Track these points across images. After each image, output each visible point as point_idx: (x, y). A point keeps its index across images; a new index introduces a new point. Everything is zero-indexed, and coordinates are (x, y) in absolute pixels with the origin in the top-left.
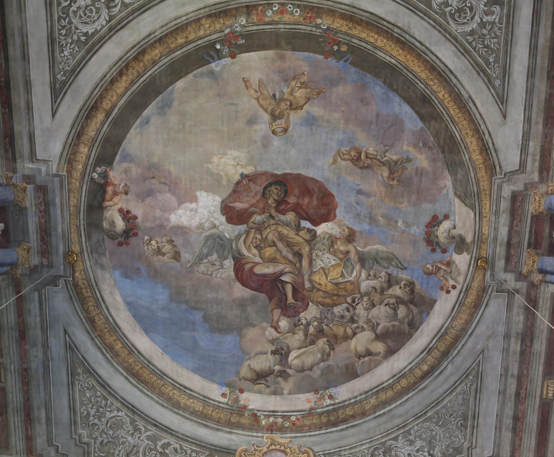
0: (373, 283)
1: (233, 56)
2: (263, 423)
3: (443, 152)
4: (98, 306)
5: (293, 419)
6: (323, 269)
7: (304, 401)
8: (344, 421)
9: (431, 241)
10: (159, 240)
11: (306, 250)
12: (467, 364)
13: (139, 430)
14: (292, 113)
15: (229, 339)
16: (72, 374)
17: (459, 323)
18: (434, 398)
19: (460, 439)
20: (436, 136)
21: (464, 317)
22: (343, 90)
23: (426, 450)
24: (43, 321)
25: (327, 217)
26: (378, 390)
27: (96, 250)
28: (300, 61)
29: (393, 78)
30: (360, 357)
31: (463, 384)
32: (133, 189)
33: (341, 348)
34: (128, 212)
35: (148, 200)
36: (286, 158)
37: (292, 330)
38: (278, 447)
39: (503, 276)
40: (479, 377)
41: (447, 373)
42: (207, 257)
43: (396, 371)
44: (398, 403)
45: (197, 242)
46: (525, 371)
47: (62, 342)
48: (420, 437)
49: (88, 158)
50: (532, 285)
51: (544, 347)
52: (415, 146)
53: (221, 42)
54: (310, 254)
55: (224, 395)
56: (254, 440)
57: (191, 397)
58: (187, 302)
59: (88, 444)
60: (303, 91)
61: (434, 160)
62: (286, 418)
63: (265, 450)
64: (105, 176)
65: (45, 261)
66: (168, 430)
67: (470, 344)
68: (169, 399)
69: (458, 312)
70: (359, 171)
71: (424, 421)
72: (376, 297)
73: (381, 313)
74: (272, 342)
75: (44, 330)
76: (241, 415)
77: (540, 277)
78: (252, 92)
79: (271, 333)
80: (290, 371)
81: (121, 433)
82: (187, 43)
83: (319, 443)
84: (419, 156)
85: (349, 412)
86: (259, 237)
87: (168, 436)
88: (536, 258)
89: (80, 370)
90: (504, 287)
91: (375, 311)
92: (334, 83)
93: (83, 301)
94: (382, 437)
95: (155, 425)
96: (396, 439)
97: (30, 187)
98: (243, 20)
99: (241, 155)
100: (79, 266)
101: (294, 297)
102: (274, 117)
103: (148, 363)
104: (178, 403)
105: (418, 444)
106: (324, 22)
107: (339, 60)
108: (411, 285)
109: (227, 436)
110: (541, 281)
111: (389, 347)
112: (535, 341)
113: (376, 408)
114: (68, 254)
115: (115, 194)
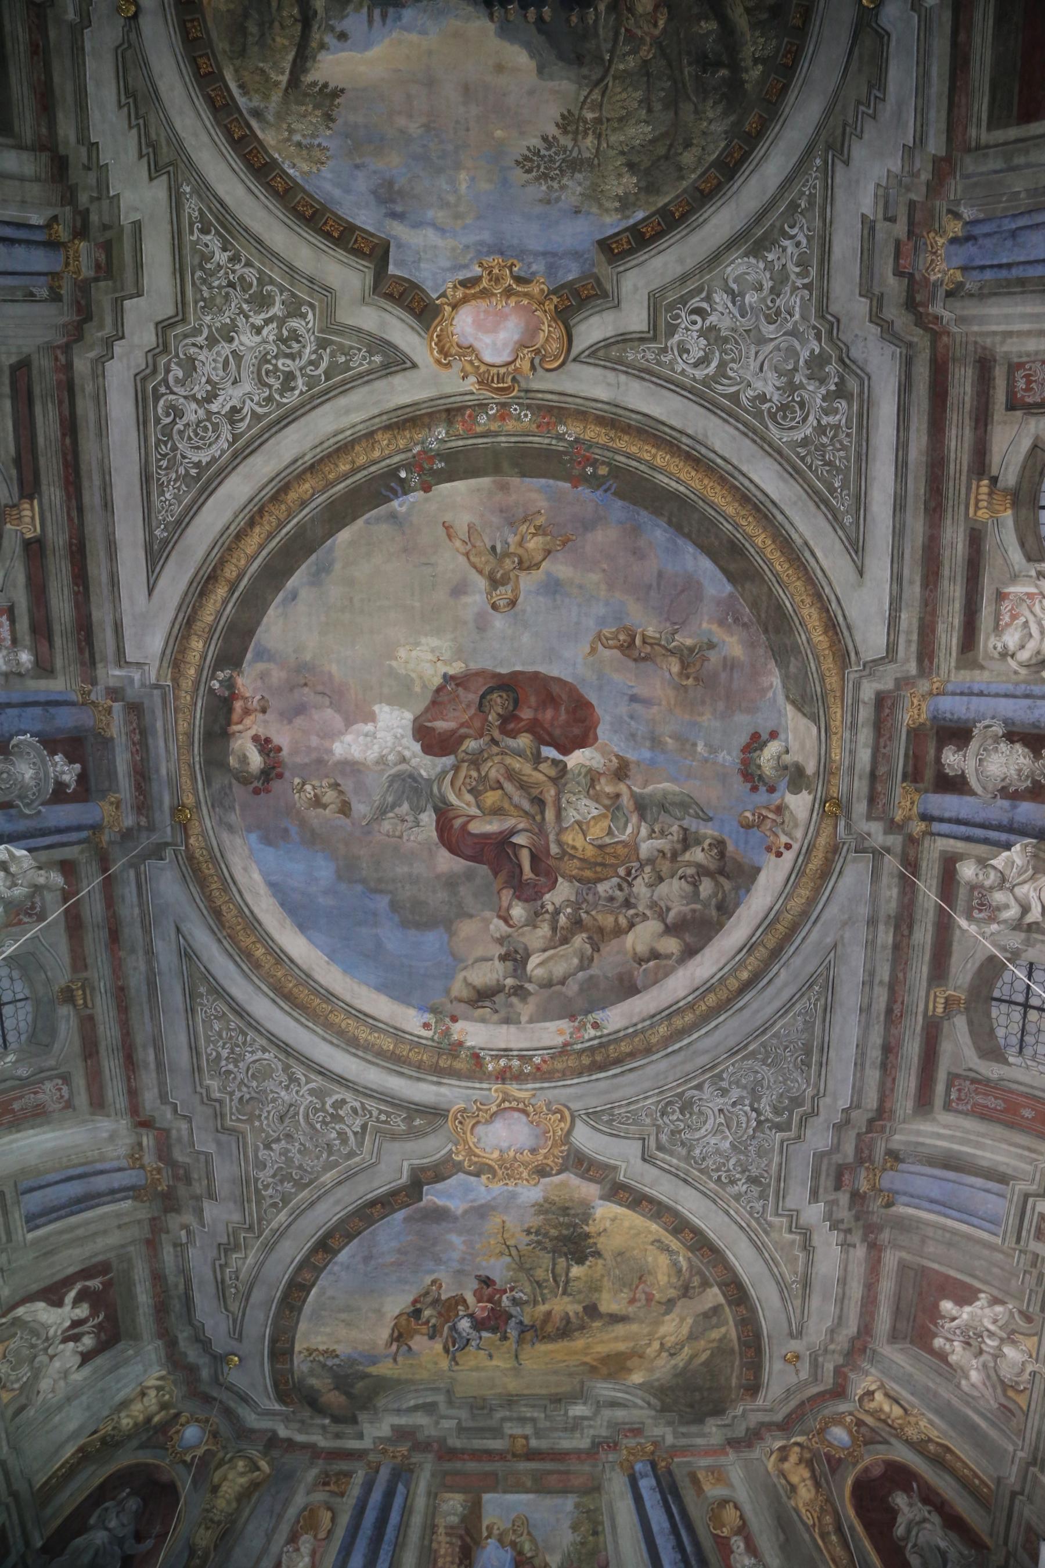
1: (427, 489)
2: (490, 1067)
3: (766, 631)
4: (225, 889)
5: (537, 1060)
6: (578, 823)
7: (553, 1033)
8: (618, 1061)
9: (750, 774)
10: (316, 783)
12: (810, 969)
13: (297, 1080)
14: (523, 575)
15: (432, 939)
16: (191, 995)
17: (796, 904)
18: (759, 1022)
19: (799, 1084)
20: (754, 605)
21: (805, 893)
22: (604, 537)
24: (144, 914)
25: (583, 741)
26: (671, 1012)
27: (220, 802)
28: (533, 493)
30: (640, 961)
32: (274, 703)
33: (610, 948)
34: (268, 740)
35: (299, 721)
37: (532, 922)
38: (514, 1104)
39: (864, 826)
41: (778, 982)
42: (393, 807)
43: (697, 982)
45: (377, 786)
46: (901, 975)
47: (174, 946)
48: (737, 1083)
50: (911, 840)
52: (722, 623)
53: (408, 467)
55: (426, 1026)
56: (476, 1095)
57: (374, 1029)
58: (363, 881)
59: (220, 1102)
60: (540, 539)
61: (752, 645)
63: (494, 1108)
64: (230, 684)
65: (143, 821)
66: (341, 1081)
67: (814, 936)
68: (341, 1033)
69: (796, 885)
70: (631, 664)
71: (744, 1058)
72: (665, 867)
73: (673, 890)
74: (501, 941)
75: (146, 930)
76: (455, 1057)
77: (922, 826)
78: (458, 543)
79: (498, 927)
82: (354, 471)
83: (579, 1097)
84: (728, 639)
85: (625, 1047)
86: (474, 774)
87: (342, 1090)
88: (916, 797)
89: (202, 990)
90: (866, 844)
91: (663, 889)
92: (588, 525)
93: (202, 882)
95: (320, 1073)
96: (699, 1087)
97: (117, 707)
98: (441, 432)
99: (443, 644)
100: (195, 828)
101: (533, 869)
102: (495, 583)
103: (307, 978)
105: (735, 1093)
106: (570, 430)
107: (595, 488)
108: (720, 844)
109: (434, 1088)
110: (925, 833)
111: (687, 945)
112: (916, 928)
113: (667, 1041)
114: (178, 808)
115: (247, 712)
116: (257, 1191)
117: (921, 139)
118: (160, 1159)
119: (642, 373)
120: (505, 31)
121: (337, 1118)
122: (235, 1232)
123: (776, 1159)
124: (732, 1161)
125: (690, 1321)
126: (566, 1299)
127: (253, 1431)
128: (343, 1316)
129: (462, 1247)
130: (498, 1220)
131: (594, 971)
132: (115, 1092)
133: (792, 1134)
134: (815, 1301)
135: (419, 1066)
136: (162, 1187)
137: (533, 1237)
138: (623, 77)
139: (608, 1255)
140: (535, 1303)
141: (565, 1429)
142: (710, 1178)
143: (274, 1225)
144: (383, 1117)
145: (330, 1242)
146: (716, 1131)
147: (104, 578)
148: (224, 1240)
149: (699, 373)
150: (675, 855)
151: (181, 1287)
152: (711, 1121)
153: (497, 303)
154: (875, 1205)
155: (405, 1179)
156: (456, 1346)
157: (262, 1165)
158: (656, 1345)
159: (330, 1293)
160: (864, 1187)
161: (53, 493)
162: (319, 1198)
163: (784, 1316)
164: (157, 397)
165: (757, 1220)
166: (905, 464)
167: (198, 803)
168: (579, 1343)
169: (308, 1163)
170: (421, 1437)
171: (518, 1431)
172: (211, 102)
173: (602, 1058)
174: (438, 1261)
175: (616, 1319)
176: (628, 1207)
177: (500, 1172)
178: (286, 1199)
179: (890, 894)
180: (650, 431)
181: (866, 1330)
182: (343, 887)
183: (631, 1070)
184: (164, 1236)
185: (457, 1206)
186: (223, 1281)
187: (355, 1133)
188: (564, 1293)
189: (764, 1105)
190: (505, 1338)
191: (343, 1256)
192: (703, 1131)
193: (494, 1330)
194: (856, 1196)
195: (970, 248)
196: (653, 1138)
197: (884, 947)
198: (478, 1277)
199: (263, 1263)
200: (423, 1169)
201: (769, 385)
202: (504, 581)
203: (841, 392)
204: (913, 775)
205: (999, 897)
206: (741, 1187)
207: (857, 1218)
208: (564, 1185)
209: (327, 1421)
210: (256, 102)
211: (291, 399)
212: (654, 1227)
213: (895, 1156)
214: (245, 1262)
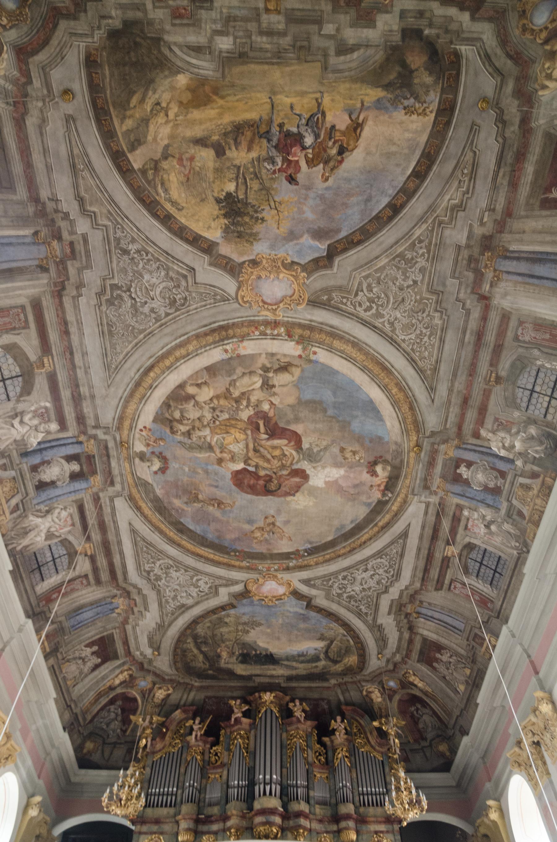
0: (201, 434)
2: (282, 330)
4: (404, 419)
5: (257, 333)
6: (238, 442)
7: (248, 348)
8: (213, 331)
9: (163, 458)
11: (251, 454)
12: (119, 376)
13: (389, 323)
14: (262, 525)
15: (308, 395)
16: (435, 370)
18: (140, 349)
19: (111, 313)
20: (171, 515)
23: (139, 304)
25: (238, 473)
26: (187, 356)
27: (398, 453)
29: (203, 541)
30: (205, 383)
31: (118, 361)
32: (366, 488)
35: (357, 482)
36: (266, 504)
37: (259, 402)
38: (270, 307)
40: (107, 367)
41: (134, 370)
42: (321, 450)
43: (176, 372)
44: (169, 346)
46: (71, 373)
47: (437, 393)
49: (393, 504)
50: (84, 433)
51: (63, 394)
52: (183, 510)
53: (304, 556)
54: (248, 451)
55: (315, 353)
56: (290, 314)
58: (338, 421)
59: (436, 310)
61: (170, 503)
62: (264, 334)
63: (281, 305)
64: (384, 495)
66: (365, 323)
67: (120, 392)
68: (360, 350)
69: (134, 414)
71: (145, 330)
72: (197, 424)
73: (193, 414)
75: (449, 402)
76: (301, 336)
79: (276, 400)
80: (261, 372)
81: (405, 321)
83: (234, 310)
85: (210, 339)
89: (429, 372)
90: (104, 430)
92: (238, 539)
93: (416, 422)
94: (179, 316)
95: (375, 327)
98: (291, 564)
99: (293, 506)
100: (412, 444)
102: (273, 524)
103: (373, 378)
104: (353, 347)
105: (146, 309)
106: (244, 564)
108: (173, 432)
109: (314, 318)
110: (78, 436)
112: (70, 396)
115: (379, 486)
116: (429, 252)
117: (134, 628)
118: (482, 274)
119: (220, 578)
120: (267, 650)
121: (371, 301)
122: (450, 222)
123: (114, 265)
124: (141, 266)
125: (150, 138)
126: (237, 162)
127: (490, 19)
128: (393, 149)
129: (305, 208)
130: (281, 229)
131: (228, 379)
132: (494, 319)
133: (108, 282)
134: (63, 150)
135: (321, 331)
136: (488, 254)
137: (260, 216)
138: (230, 640)
139: (212, 200)
140: (258, 159)
141: (235, 19)
142: (152, 255)
143: (424, 226)
144: (345, 301)
145: (391, 213)
146: (153, 286)
147: (426, 529)
148: (461, 214)
149: (199, 577)
150: (194, 428)
151: (501, 174)
152: (158, 293)
153: (270, 595)
154: (44, 232)
155: (337, 260)
156: (314, 120)
157: (422, 270)
158: (171, 115)
159: (399, 170)
160: (55, 243)
161: (438, 556)
162: (392, 247)
163: (83, 138)
164: (393, 576)
165: (118, 223)
166: (120, 554)
167: (408, 453)
168: (227, 119)
169: (393, 272)
170: (353, 12)
171: (274, 18)
172: (358, 638)
173: (222, 333)
174: (322, 197)
175: (201, 142)
176: (201, 236)
177: (280, 264)
178: (413, 246)
179: (87, 409)
180: (217, 564)
181: (20, 123)
182: (348, 419)
183: (206, 326)
184: (499, 218)
185: (307, 240)
186: (470, 180)
187: (362, 291)
188: (239, 168)
189: (129, 303)
190: (281, 126)
191: (385, 201)
192: (161, 287)
193: (288, 134)
194: (59, 238)
195: (111, 607)
196: (190, 284)
197: (83, 385)
198: (297, 184)
199: (439, 195)
200: (325, 267)
201: (174, 574)
202: (269, 524)
203: (148, 573)
204: (90, 458)
205: (36, 422)
206: (133, 248)
207: (53, 220)
208: (241, 254)
209: (426, 32)
211: (345, 573)
212: (183, 221)
213: (44, 269)
214: (452, 196)
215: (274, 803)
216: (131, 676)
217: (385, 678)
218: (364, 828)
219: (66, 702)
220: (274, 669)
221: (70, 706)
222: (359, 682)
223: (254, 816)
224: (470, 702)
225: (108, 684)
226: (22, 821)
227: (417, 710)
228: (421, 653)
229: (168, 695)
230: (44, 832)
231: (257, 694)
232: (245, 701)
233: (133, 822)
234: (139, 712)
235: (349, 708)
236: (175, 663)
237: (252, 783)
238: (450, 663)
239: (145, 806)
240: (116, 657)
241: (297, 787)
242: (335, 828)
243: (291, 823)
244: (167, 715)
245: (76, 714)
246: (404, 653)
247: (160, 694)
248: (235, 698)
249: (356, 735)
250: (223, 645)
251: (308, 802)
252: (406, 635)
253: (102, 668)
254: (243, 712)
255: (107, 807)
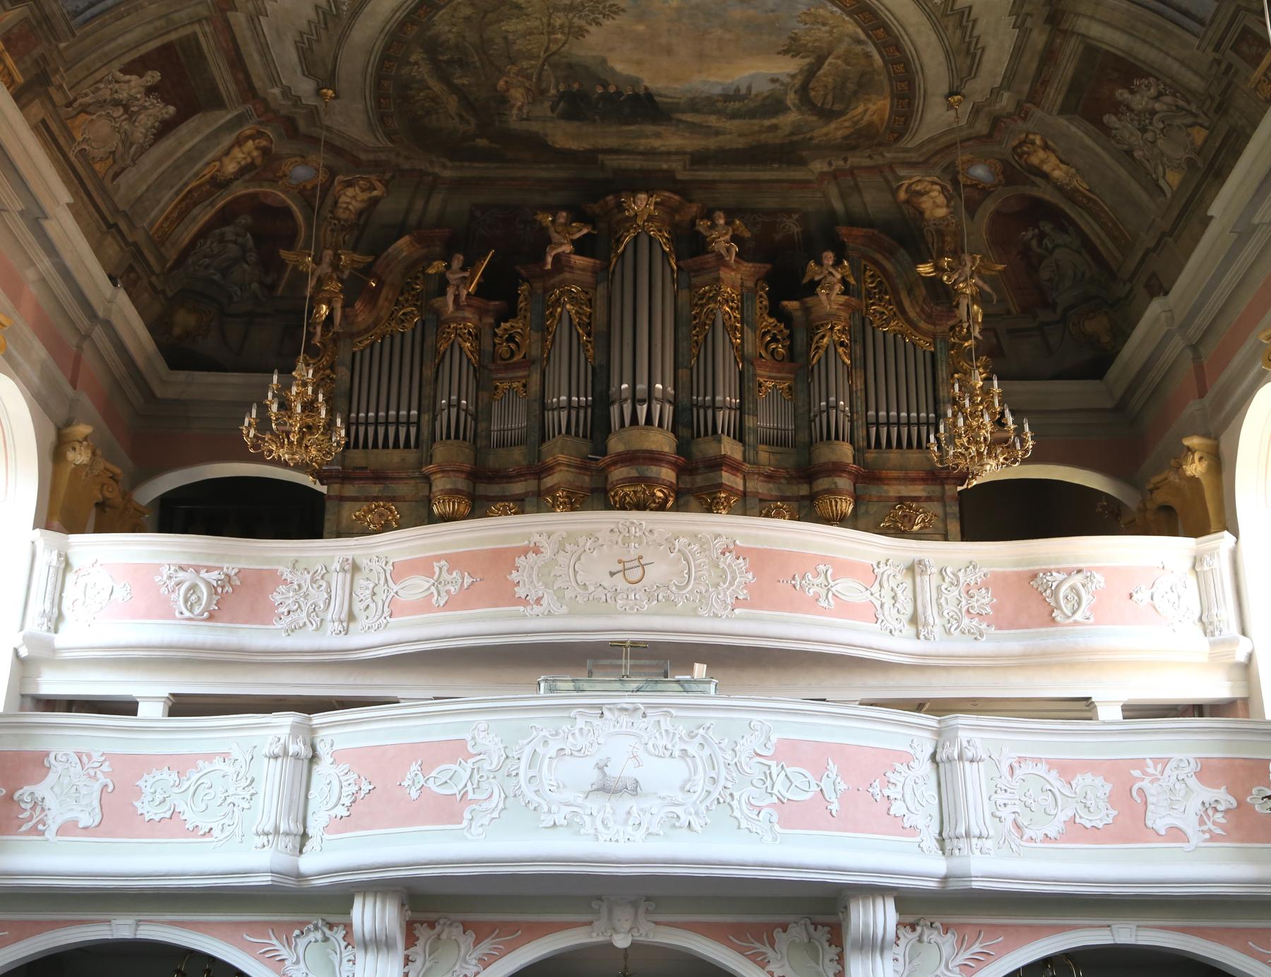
117: (253, 20)
120: (635, 82)
138: (531, 57)
172: (898, 47)
210: (858, 49)
215: (662, 441)
216: (265, 151)
217: (961, 157)
218: (874, 491)
219: (104, 216)
220: (658, 135)
221: (115, 225)
222: (891, 167)
223: (609, 465)
224: (1189, 215)
225: (208, 173)
226: (55, 474)
227: (1042, 236)
228: (1075, 87)
229: (374, 201)
230: (113, 494)
231: (610, 198)
232: (579, 215)
233: (321, 476)
234: (300, 244)
235: (856, 231)
236: (382, 118)
237: (603, 401)
238: (1153, 113)
239: (347, 445)
240: (215, 101)
241: (715, 408)
242: (804, 490)
243: (700, 480)
244: (378, 247)
245: (135, 244)
246: (1027, 87)
247: (352, 199)
248: (553, 210)
249: (869, 295)
250: (515, 69)
251: (740, 437)
252: (1039, 39)
253: (184, 129)
254: (573, 242)
255: (256, 447)
